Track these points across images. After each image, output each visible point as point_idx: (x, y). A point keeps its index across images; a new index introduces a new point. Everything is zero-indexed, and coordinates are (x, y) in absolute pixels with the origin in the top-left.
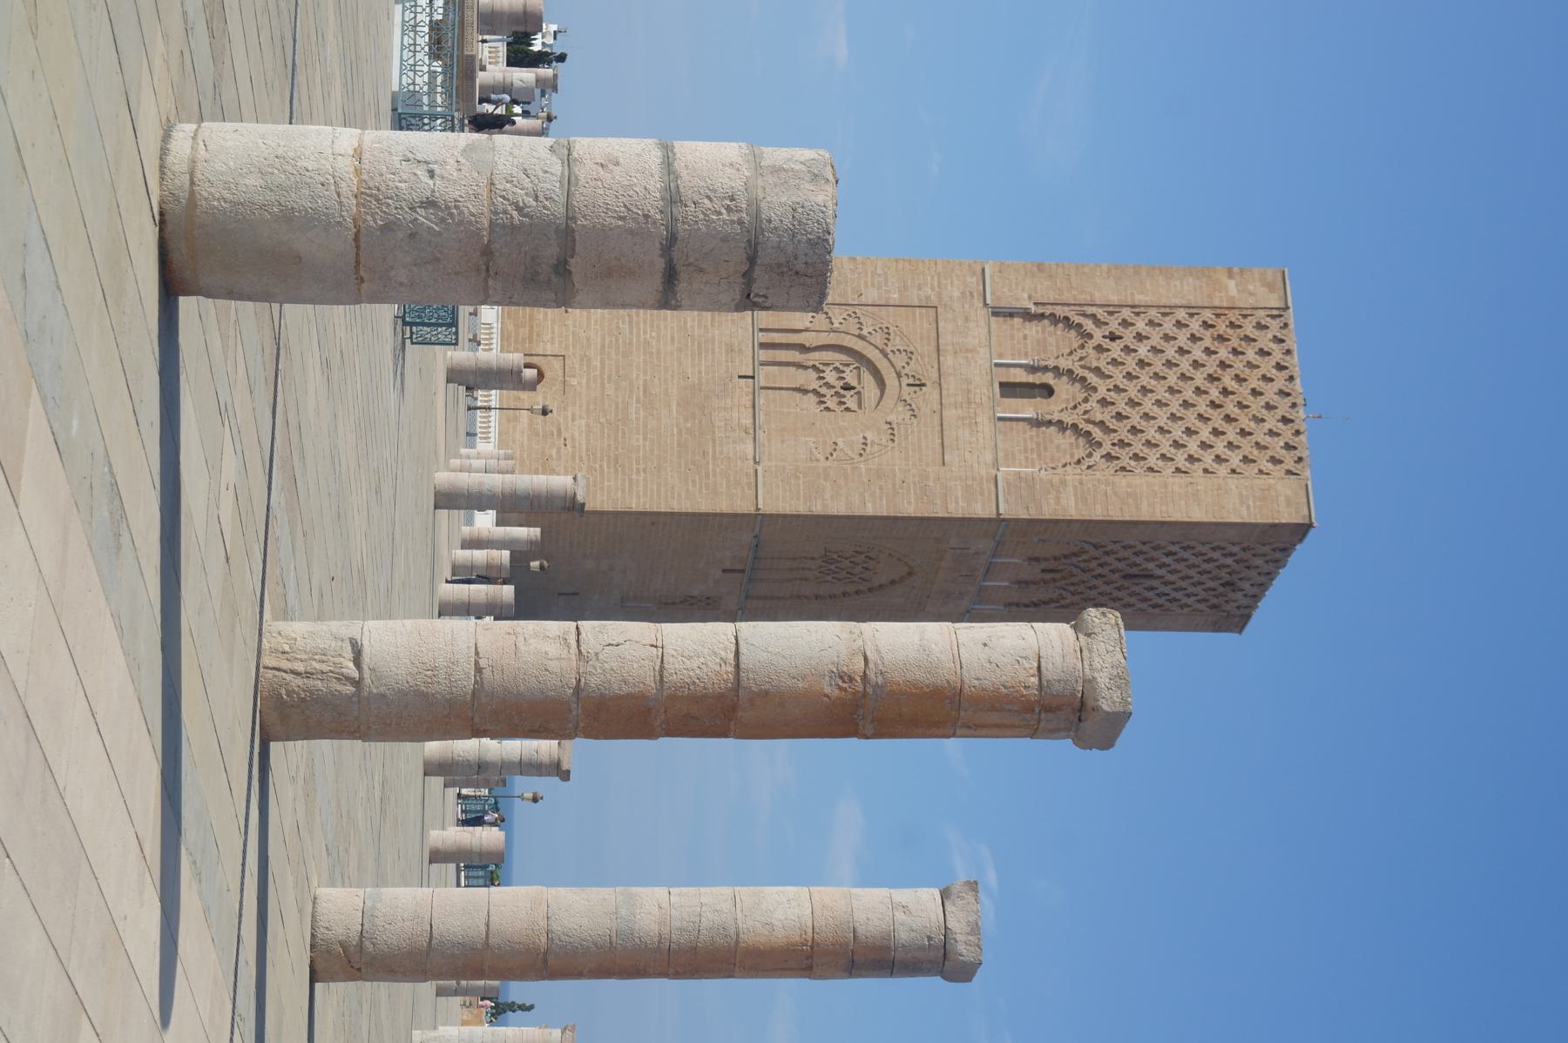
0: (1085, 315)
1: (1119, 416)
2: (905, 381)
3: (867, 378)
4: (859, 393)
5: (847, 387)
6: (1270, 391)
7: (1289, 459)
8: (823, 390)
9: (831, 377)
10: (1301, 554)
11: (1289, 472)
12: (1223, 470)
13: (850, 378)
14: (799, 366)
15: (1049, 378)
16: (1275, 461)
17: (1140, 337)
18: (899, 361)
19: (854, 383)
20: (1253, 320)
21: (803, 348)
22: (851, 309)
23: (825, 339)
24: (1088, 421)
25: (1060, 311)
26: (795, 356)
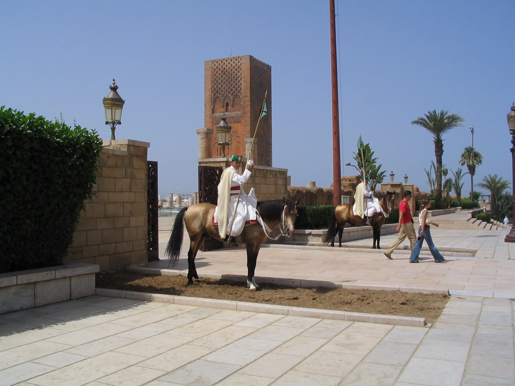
1: (232, 90)
6: (227, 63)
7: (238, 60)
10: (256, 57)
17: (217, 87)
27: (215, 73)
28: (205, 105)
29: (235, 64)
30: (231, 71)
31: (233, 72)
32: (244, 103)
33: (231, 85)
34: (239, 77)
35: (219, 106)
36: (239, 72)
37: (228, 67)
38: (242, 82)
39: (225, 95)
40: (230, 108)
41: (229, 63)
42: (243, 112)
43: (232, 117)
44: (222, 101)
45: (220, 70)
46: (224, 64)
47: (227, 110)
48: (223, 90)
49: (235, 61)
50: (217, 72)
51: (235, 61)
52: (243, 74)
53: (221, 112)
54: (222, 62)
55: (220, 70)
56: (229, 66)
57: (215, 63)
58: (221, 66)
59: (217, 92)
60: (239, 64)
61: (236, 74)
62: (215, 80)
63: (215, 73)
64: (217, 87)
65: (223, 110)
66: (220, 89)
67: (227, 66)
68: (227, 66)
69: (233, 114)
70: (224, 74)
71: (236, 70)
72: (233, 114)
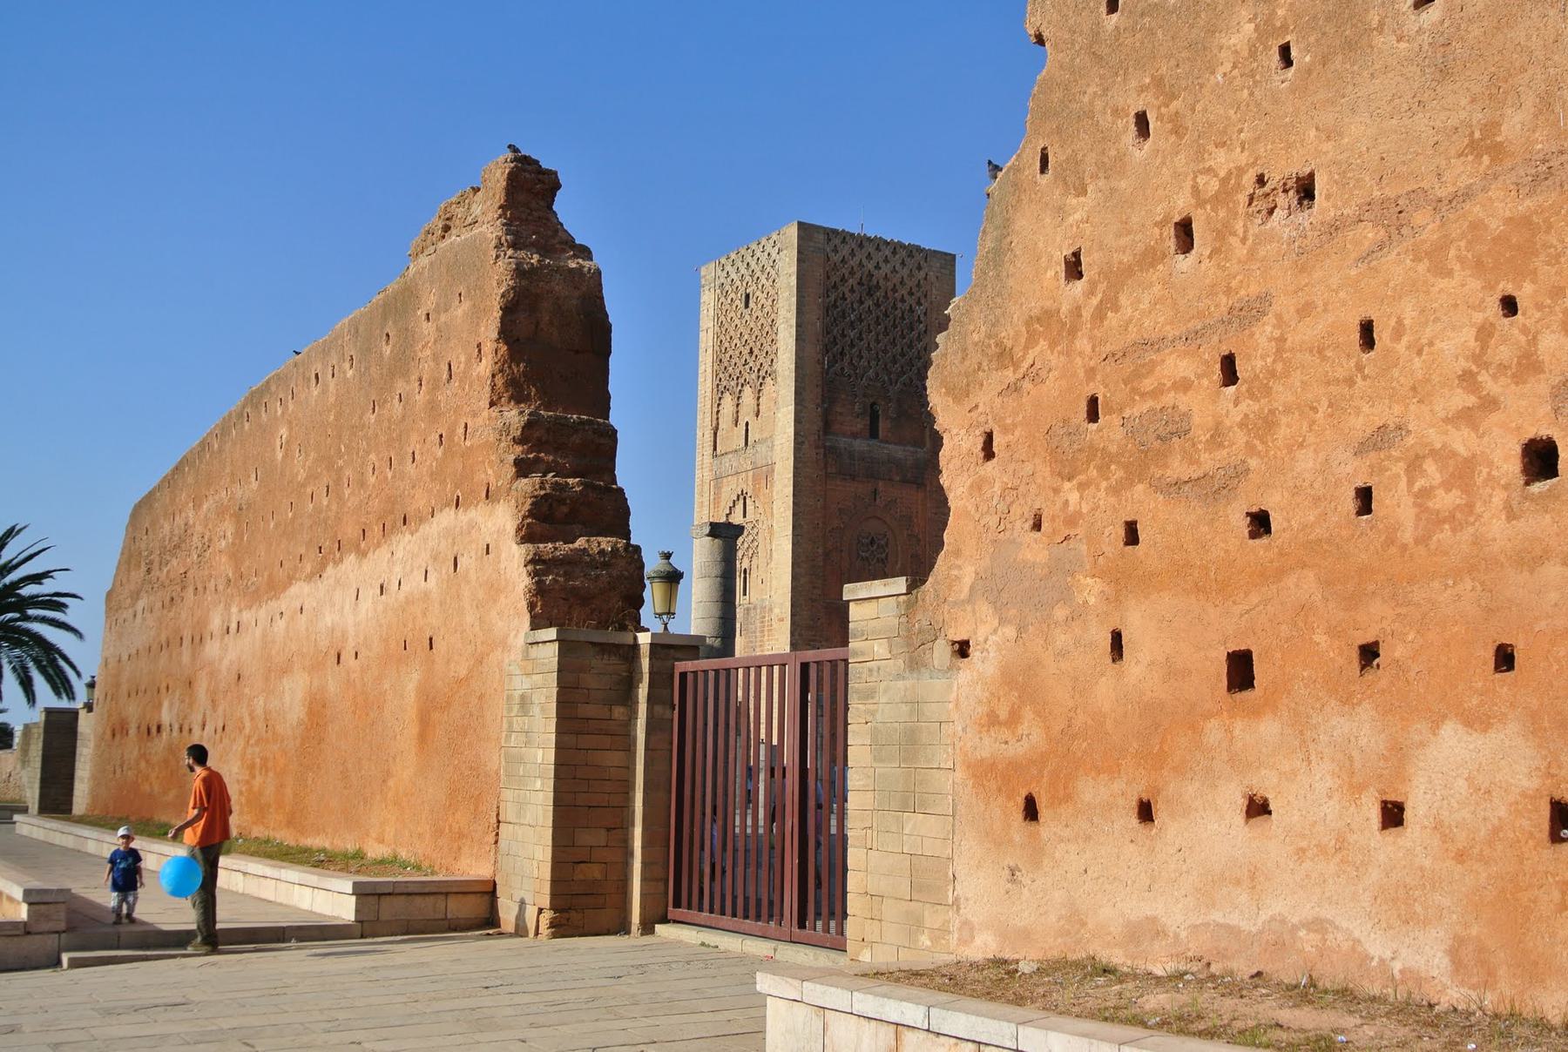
5: (872, 542)
12: (926, 305)
16: (919, 268)
20: (832, 255)
27: (834, 279)
30: (894, 290)
33: (894, 343)
36: (919, 303)
37: (882, 272)
39: (871, 373)
40: (883, 425)
41: (886, 261)
45: (852, 273)
46: (869, 257)
47: (874, 434)
48: (865, 353)
49: (908, 260)
50: (843, 279)
51: (908, 260)
53: (855, 436)
54: (861, 246)
55: (852, 273)
56: (886, 269)
57: (837, 241)
58: (857, 259)
60: (922, 274)
61: (911, 310)
62: (835, 306)
64: (844, 336)
65: (861, 424)
66: (852, 345)
67: (877, 267)
68: (877, 267)
69: (898, 452)
70: (870, 294)
71: (911, 293)
72: (898, 452)
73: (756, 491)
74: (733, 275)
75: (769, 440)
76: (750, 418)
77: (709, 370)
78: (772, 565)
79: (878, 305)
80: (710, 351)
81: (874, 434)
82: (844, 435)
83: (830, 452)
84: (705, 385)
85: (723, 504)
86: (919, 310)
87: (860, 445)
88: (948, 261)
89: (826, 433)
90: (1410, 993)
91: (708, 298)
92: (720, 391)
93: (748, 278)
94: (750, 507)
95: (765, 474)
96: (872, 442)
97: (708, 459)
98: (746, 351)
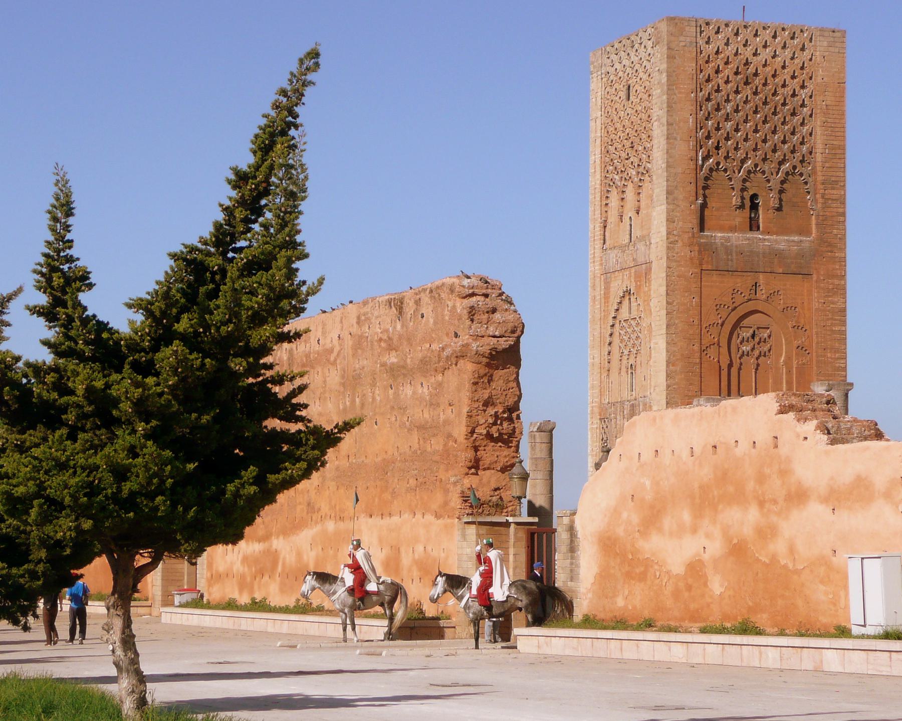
0: (703, 166)
2: (753, 296)
3: (745, 322)
4: (758, 328)
5: (753, 336)
8: (756, 353)
9: (746, 348)
11: (811, 40)
12: (810, 86)
13: (747, 334)
14: (740, 369)
15: (747, 195)
18: (739, 299)
19: (751, 331)
20: (704, 46)
21: (730, 366)
22: (704, 331)
23: (724, 350)
24: (777, 173)
25: (701, 183)
26: (734, 371)
28: (669, 193)
29: (788, 53)
31: (779, 80)
32: (825, 206)
34: (803, 105)
35: (726, 200)
37: (761, 59)
38: (817, 124)
42: (821, 240)
43: (778, 255)
44: (738, 186)
47: (753, 225)
52: (818, 99)
53: (733, 229)
56: (766, 54)
59: (718, 148)
62: (708, 99)
63: (710, 69)
69: (782, 242)
72: (782, 242)
73: (638, 288)
74: (617, 66)
75: (645, 238)
76: (632, 214)
77: (598, 162)
78: (651, 363)
79: (755, 93)
80: (598, 142)
81: (753, 225)
82: (722, 229)
83: (705, 250)
84: (595, 180)
85: (611, 299)
86: (803, 94)
87: (739, 239)
88: (837, 36)
89: (702, 229)
90: (299, 554)
91: (596, 85)
92: (608, 185)
93: (629, 70)
94: (634, 304)
95: (643, 273)
96: (750, 235)
97: (598, 253)
98: (628, 144)
